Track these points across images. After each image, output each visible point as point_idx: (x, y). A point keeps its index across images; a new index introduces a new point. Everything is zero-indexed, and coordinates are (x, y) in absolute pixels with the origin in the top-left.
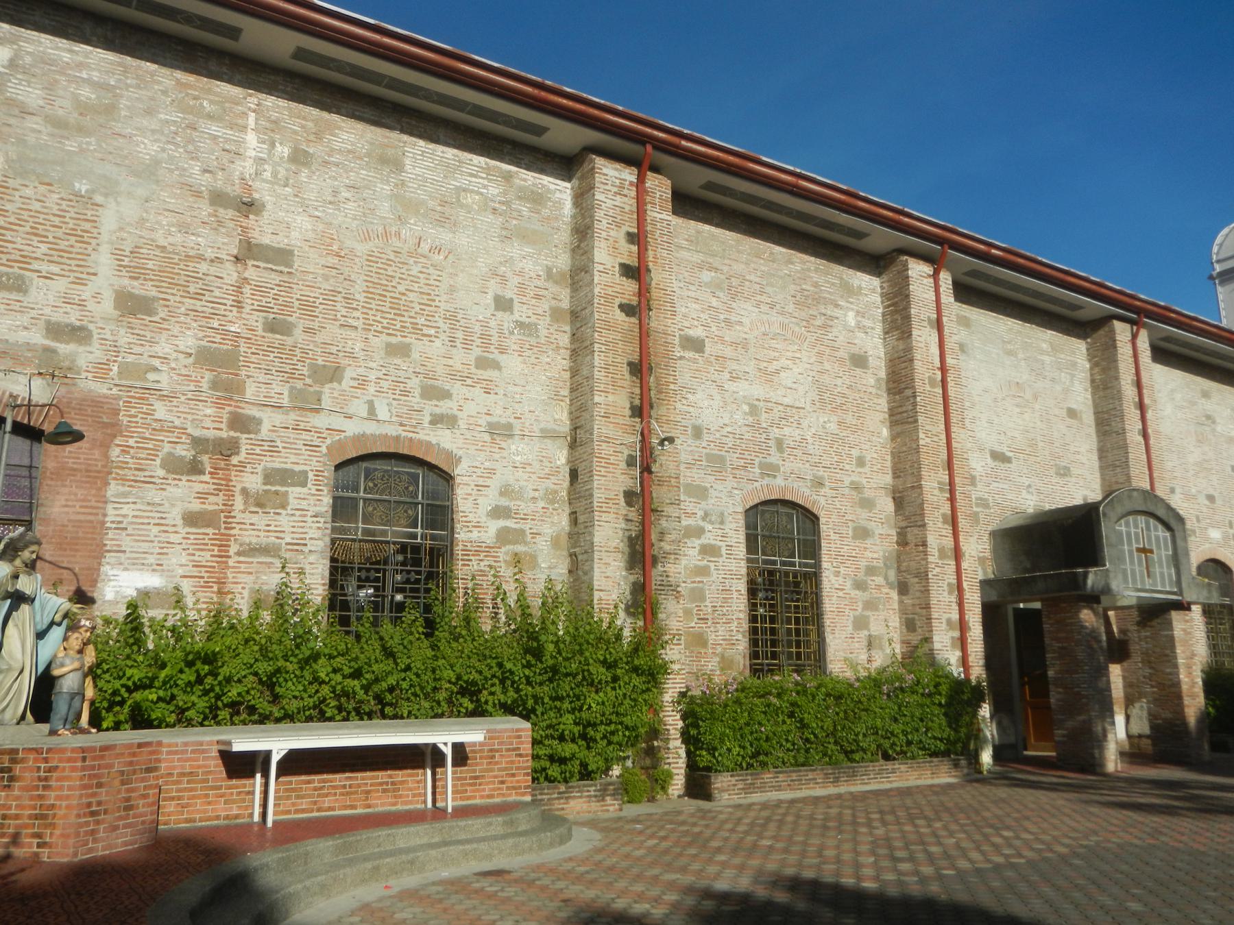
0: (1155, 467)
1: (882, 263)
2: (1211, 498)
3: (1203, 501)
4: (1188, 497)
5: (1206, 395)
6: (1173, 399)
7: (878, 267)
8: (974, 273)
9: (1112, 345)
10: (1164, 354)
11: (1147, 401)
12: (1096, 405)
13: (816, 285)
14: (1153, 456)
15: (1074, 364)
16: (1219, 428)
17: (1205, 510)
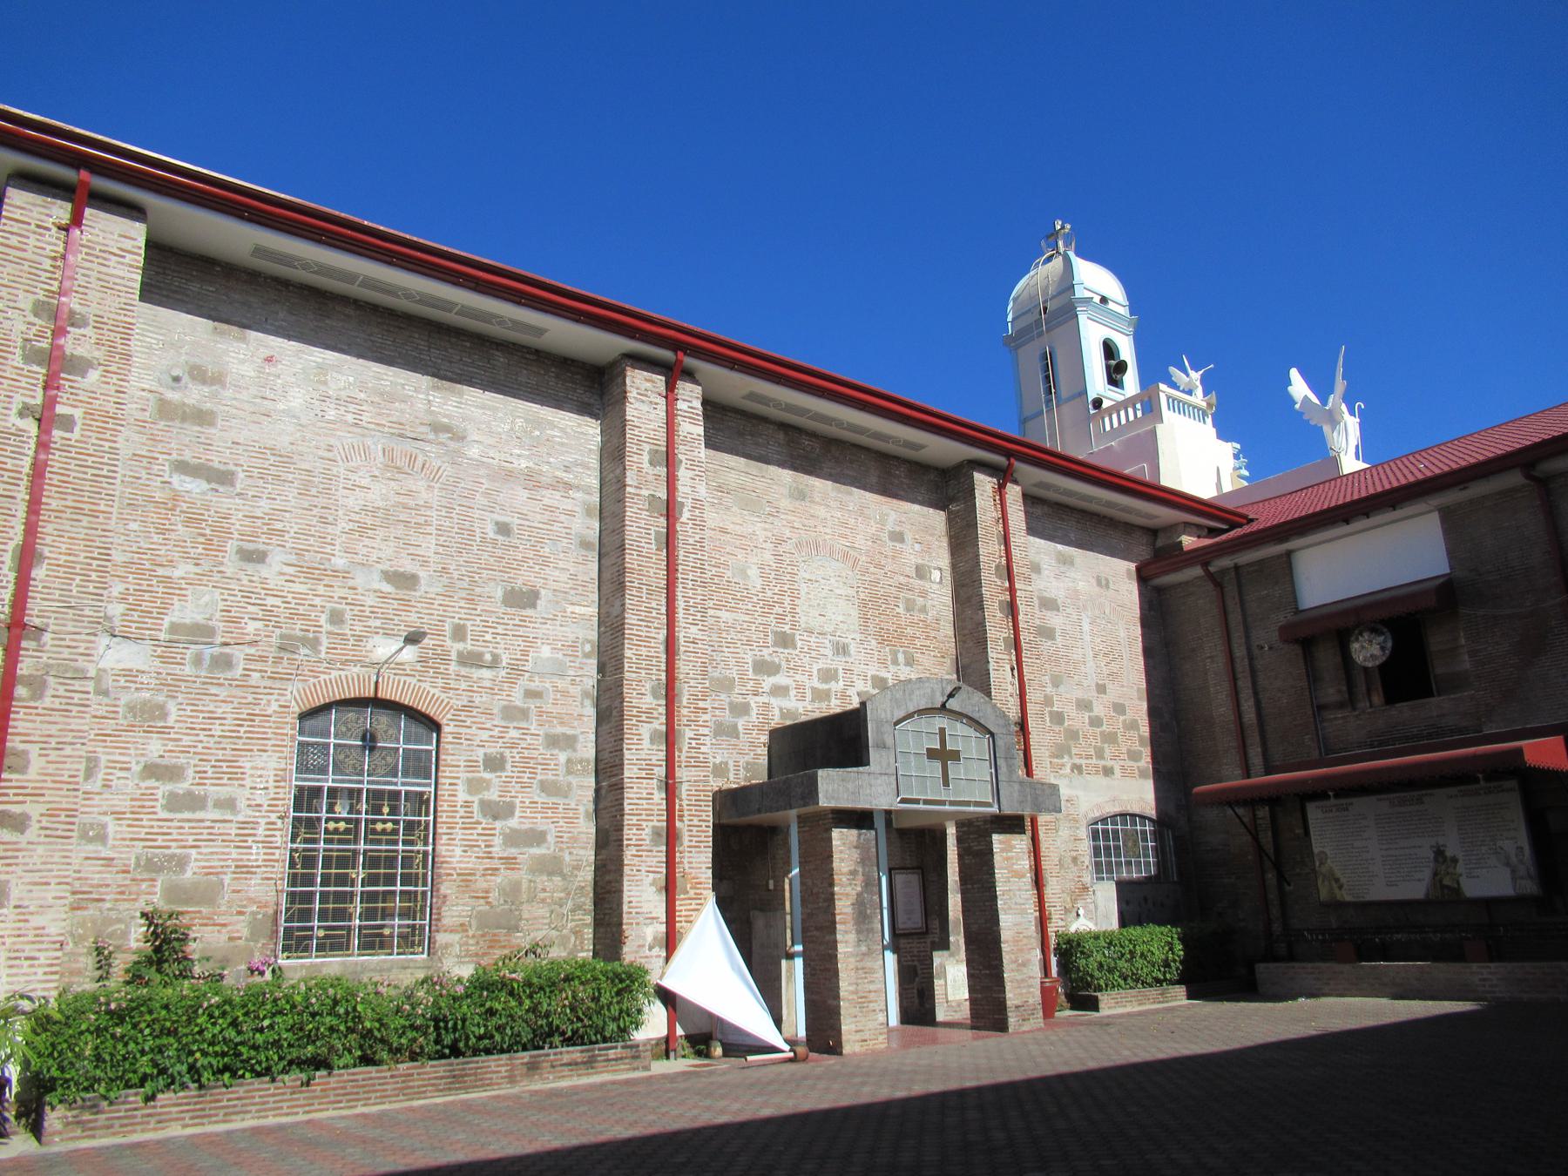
3: (370, 583)
4: (313, 572)
6: (325, 383)
17: (370, 600)
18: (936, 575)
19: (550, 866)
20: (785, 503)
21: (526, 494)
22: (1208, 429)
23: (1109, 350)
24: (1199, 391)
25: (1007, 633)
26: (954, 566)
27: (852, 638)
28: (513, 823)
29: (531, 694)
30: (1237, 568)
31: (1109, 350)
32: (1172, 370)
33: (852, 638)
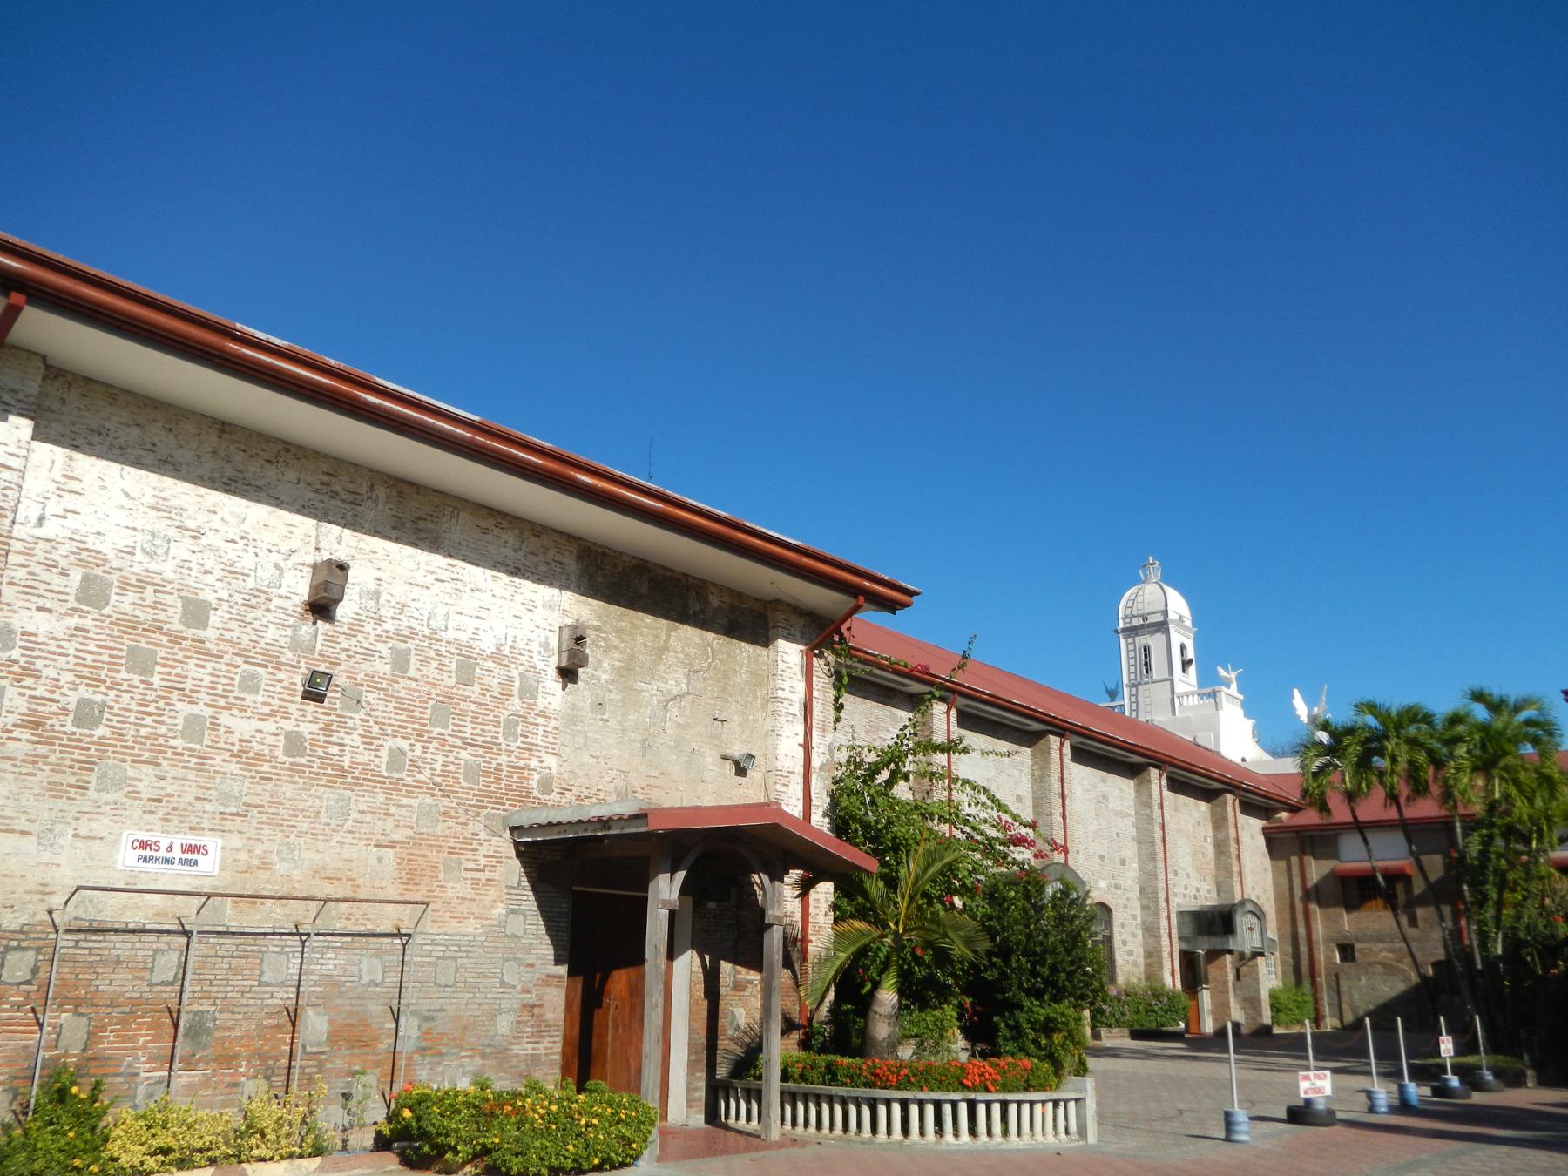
0: (1068, 839)
1: (915, 700)
2: (1102, 857)
4: (1088, 857)
5: (1104, 780)
7: (912, 702)
8: (968, 706)
9: (1047, 752)
10: (1080, 755)
11: (1066, 792)
12: (1034, 793)
13: (877, 718)
14: (1068, 831)
15: (1023, 762)
16: (1110, 805)
17: (1097, 866)
18: (1209, 840)
19: (1135, 964)
20: (1173, 813)
21: (1120, 820)
22: (1241, 712)
23: (1183, 648)
24: (1234, 686)
25: (1238, 869)
26: (1214, 836)
27: (1190, 871)
28: (1128, 948)
29: (1128, 899)
30: (1311, 836)
31: (1183, 648)
32: (1219, 669)
33: (1190, 871)
